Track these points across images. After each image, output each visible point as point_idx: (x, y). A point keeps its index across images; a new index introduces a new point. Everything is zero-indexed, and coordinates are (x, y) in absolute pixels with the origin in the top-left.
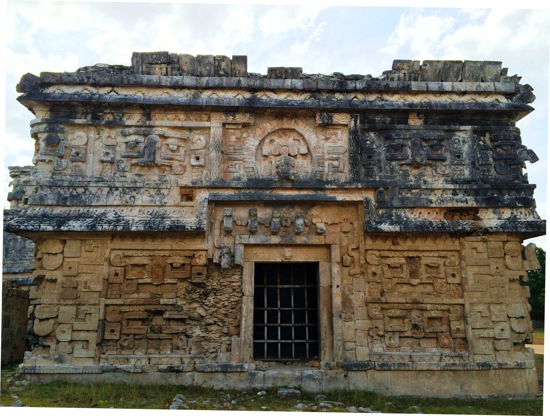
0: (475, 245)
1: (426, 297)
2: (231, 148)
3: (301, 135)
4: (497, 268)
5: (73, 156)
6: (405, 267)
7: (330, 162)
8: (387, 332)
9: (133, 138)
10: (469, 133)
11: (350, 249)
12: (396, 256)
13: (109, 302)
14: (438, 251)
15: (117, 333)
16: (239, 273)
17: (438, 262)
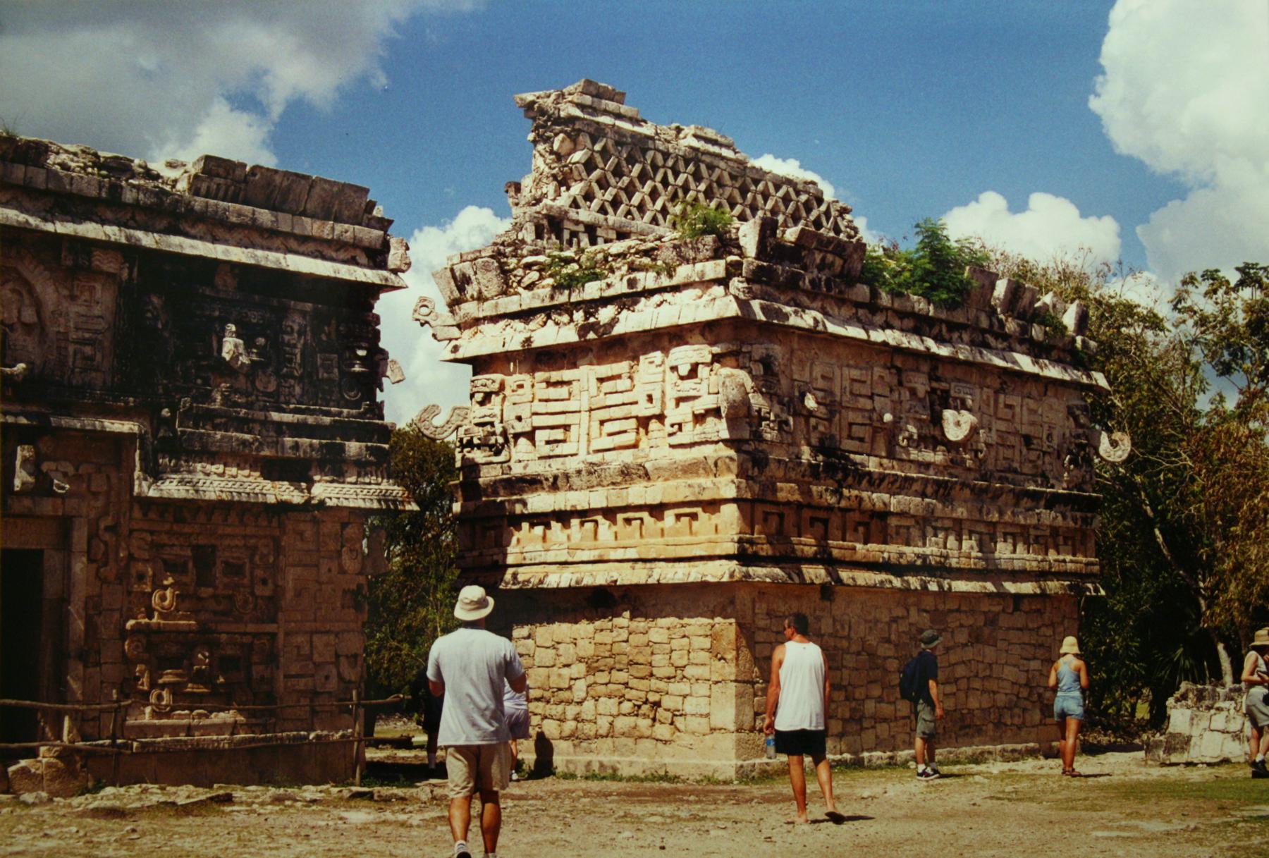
4: (330, 570)
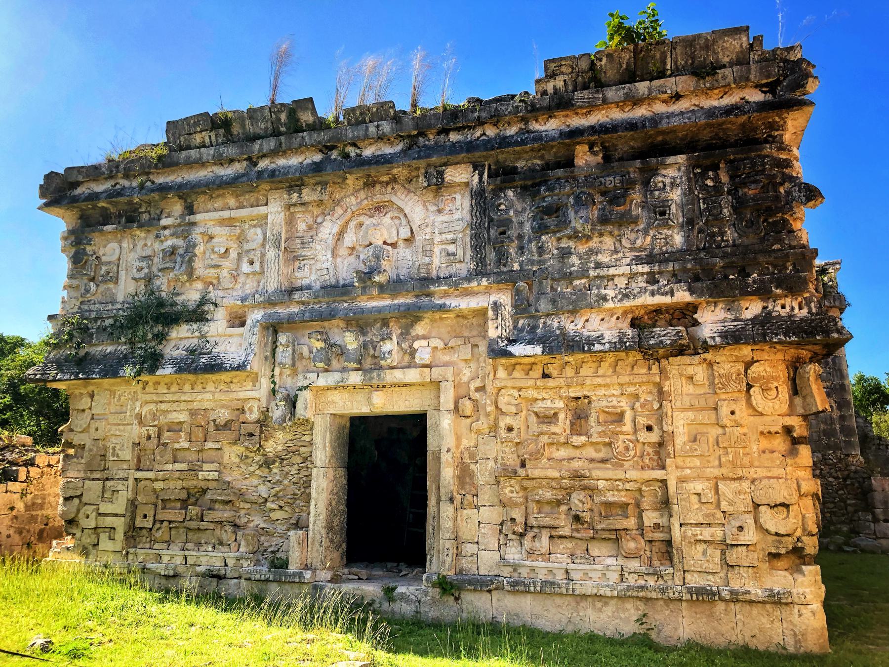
0: (690, 370)
1: (598, 469)
2: (298, 241)
3: (401, 210)
4: (733, 413)
5: (103, 276)
6: (562, 416)
7: (444, 246)
8: (532, 528)
9: (169, 243)
10: (683, 168)
11: (472, 388)
12: (546, 396)
13: (139, 475)
14: (621, 385)
15: (151, 519)
16: (310, 432)
17: (622, 404)
